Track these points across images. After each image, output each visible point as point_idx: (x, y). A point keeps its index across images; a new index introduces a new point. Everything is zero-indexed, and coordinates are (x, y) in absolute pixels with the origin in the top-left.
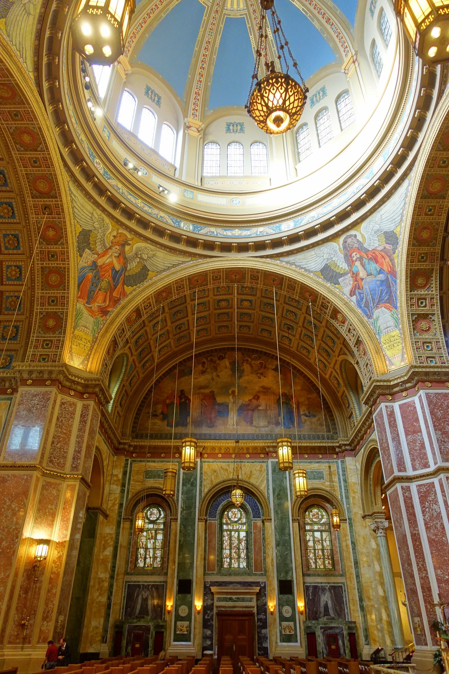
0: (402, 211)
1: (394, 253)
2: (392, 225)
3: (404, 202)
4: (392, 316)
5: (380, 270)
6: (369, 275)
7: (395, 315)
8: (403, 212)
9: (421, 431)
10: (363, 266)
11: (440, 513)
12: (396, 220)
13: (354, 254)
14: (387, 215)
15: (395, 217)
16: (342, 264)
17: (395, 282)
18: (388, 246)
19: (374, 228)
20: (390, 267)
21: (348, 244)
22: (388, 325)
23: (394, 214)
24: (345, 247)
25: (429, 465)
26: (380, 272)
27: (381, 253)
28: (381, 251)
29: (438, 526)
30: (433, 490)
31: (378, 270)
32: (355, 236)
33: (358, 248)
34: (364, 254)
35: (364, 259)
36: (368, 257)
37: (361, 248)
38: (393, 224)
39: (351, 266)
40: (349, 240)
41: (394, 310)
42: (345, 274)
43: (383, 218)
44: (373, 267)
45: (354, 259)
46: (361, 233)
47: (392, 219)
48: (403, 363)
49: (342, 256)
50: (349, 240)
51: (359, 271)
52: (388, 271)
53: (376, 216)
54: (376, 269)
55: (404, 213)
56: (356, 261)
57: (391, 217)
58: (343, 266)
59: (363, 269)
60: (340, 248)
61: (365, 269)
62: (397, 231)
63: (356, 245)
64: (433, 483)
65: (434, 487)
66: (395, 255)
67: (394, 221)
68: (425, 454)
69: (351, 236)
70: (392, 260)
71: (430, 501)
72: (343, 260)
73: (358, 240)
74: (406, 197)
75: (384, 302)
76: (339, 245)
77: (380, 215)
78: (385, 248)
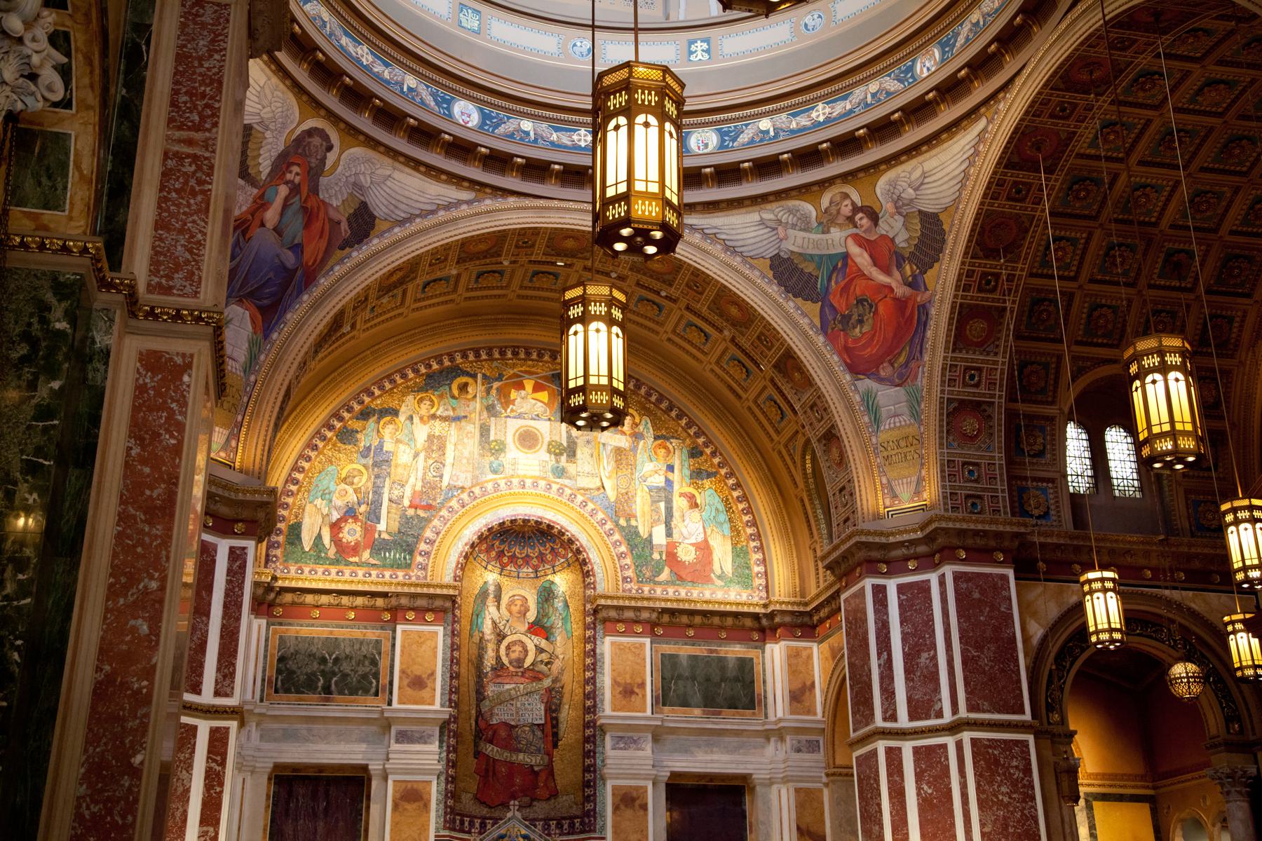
0: (418, 212)
1: (342, 248)
2: (383, 208)
3: (434, 207)
4: (252, 343)
5: (297, 245)
6: (278, 230)
7: (255, 349)
8: (418, 216)
9: (208, 615)
10: (285, 206)
11: (188, 791)
12: (398, 212)
13: (296, 169)
14: (396, 188)
15: (403, 207)
16: (265, 160)
17: (300, 293)
18: (344, 226)
19: (362, 177)
20: (315, 261)
21: (309, 143)
22: (235, 355)
23: (404, 200)
24: (299, 141)
25: (201, 690)
26: (297, 248)
27: (327, 220)
28: (331, 220)
29: (178, 814)
30: (192, 742)
31: (296, 242)
32: (330, 148)
33: (311, 168)
34: (306, 188)
35: (297, 198)
36: (305, 201)
37: (314, 173)
38: (386, 211)
39: (271, 181)
40: (316, 141)
41: (260, 336)
42: (252, 181)
43: (388, 183)
44: (295, 226)
45: (289, 176)
46: (340, 155)
47: (393, 202)
48: (223, 454)
49: (281, 148)
50: (316, 141)
51: (271, 204)
52: (307, 263)
53: (384, 166)
54: (294, 238)
55: (418, 220)
56: (287, 183)
57: (398, 197)
58: (264, 165)
59: (280, 209)
60: (293, 131)
61: (282, 214)
62: (380, 226)
63: (314, 162)
64: (195, 728)
65: (195, 736)
66: (339, 254)
67: (392, 207)
68: (201, 665)
69: (326, 137)
70: (328, 253)
71: (181, 761)
72: (275, 154)
73: (325, 158)
74: (448, 207)
75: (260, 308)
76: (298, 125)
77: (388, 173)
78: (339, 223)
